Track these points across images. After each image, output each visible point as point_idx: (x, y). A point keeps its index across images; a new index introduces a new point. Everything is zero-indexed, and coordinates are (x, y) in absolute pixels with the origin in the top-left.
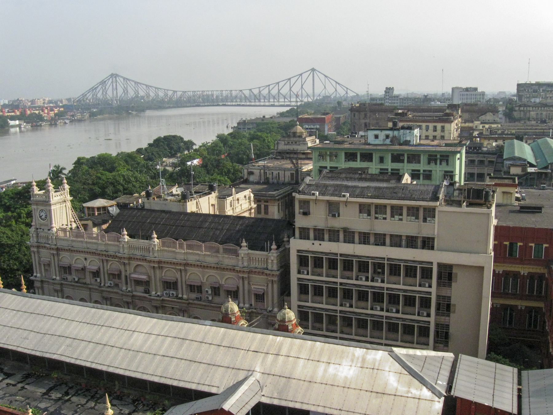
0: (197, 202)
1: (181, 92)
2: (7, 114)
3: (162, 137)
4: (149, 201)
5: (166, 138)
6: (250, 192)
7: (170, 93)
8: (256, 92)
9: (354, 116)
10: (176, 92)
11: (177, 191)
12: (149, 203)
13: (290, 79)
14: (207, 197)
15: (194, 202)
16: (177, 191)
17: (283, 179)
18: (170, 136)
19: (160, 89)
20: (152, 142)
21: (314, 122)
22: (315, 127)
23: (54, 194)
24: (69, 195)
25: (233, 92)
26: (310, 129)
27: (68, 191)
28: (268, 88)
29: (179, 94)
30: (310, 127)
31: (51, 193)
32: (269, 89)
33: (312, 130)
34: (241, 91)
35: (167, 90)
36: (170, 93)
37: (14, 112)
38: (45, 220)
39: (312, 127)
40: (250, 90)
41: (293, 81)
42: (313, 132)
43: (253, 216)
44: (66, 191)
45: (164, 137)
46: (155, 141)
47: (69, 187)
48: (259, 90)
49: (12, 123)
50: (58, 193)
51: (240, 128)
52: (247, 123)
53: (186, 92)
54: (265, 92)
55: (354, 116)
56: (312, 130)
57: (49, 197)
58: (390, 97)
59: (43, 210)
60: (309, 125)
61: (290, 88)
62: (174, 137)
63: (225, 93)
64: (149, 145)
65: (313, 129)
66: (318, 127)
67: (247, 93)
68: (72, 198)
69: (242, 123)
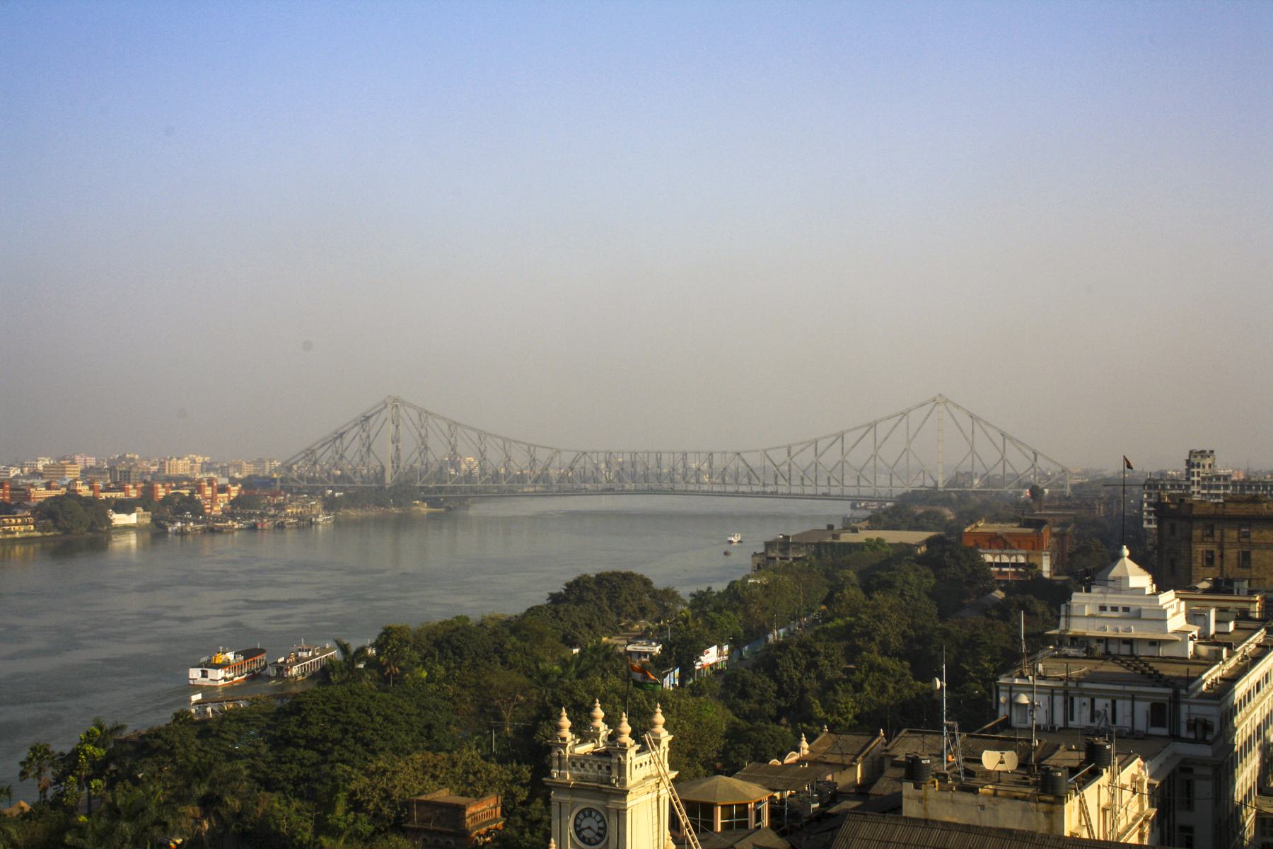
0: (1080, 801)
1: (572, 455)
2: (103, 496)
3: (593, 576)
4: (917, 791)
5: (601, 579)
6: (1139, 766)
7: (542, 456)
8: (780, 457)
9: (1173, 532)
10: (559, 451)
11: (1002, 762)
12: (921, 799)
13: (873, 425)
14: (1095, 785)
15: (1076, 799)
16: (1002, 762)
17: (1128, 722)
18: (614, 574)
19: (515, 442)
20: (559, 588)
21: (1011, 548)
22: (1013, 560)
23: (638, 760)
24: (667, 766)
25: (716, 458)
26: (997, 565)
27: (667, 750)
28: (813, 445)
29: (567, 458)
30: (997, 560)
31: (628, 755)
32: (816, 450)
33: (1004, 569)
34: (738, 454)
35: (535, 446)
36: (542, 456)
37: (122, 489)
38: (597, 843)
39: (1005, 559)
40: (765, 451)
41: (882, 430)
42: (1006, 573)
43: (1146, 842)
44: (662, 751)
45: (598, 576)
46: (570, 587)
47: (671, 737)
48: (789, 453)
49: (119, 519)
50: (645, 757)
51: (774, 558)
52: (792, 543)
53: (585, 453)
54: (805, 458)
55: (1173, 532)
56: (1004, 569)
57: (621, 768)
58: (1204, 479)
59: (590, 810)
60: (994, 555)
61: (876, 448)
62: (627, 577)
63: (805, 459)
64: (555, 599)
65: (1006, 565)
66: (1022, 560)
67: (755, 460)
68: (673, 774)
69: (780, 543)
